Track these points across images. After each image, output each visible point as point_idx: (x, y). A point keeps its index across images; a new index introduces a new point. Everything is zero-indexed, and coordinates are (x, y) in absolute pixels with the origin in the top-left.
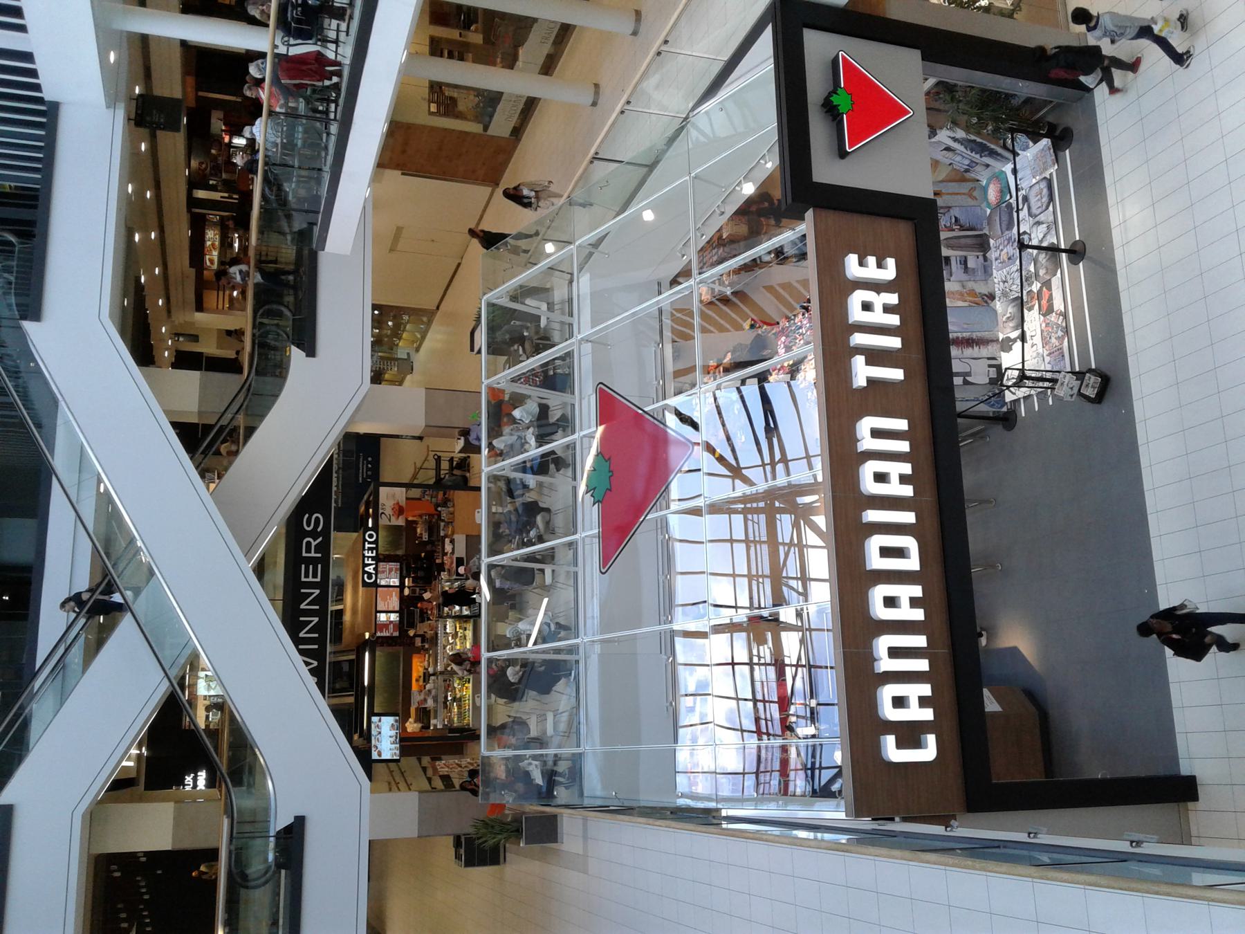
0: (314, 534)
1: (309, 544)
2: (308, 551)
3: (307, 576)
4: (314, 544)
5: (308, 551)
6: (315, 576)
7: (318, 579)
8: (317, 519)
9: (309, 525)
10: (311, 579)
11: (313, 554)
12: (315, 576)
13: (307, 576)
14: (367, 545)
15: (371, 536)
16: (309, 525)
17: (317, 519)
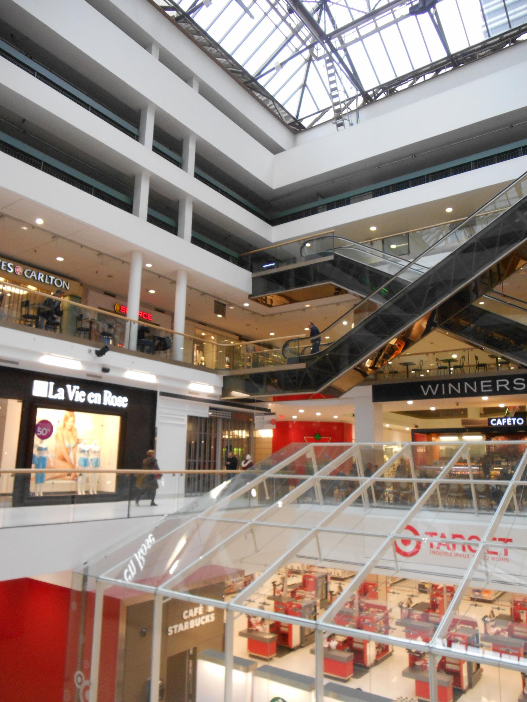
0: (511, 385)
1: (505, 383)
2: (500, 383)
3: (484, 384)
4: (505, 386)
5: (500, 383)
6: (485, 388)
7: (482, 390)
8: (522, 386)
9: (517, 381)
10: (482, 386)
11: (498, 386)
12: (485, 388)
13: (484, 384)
14: (514, 419)
15: (520, 421)
16: (517, 381)
17: (522, 386)
